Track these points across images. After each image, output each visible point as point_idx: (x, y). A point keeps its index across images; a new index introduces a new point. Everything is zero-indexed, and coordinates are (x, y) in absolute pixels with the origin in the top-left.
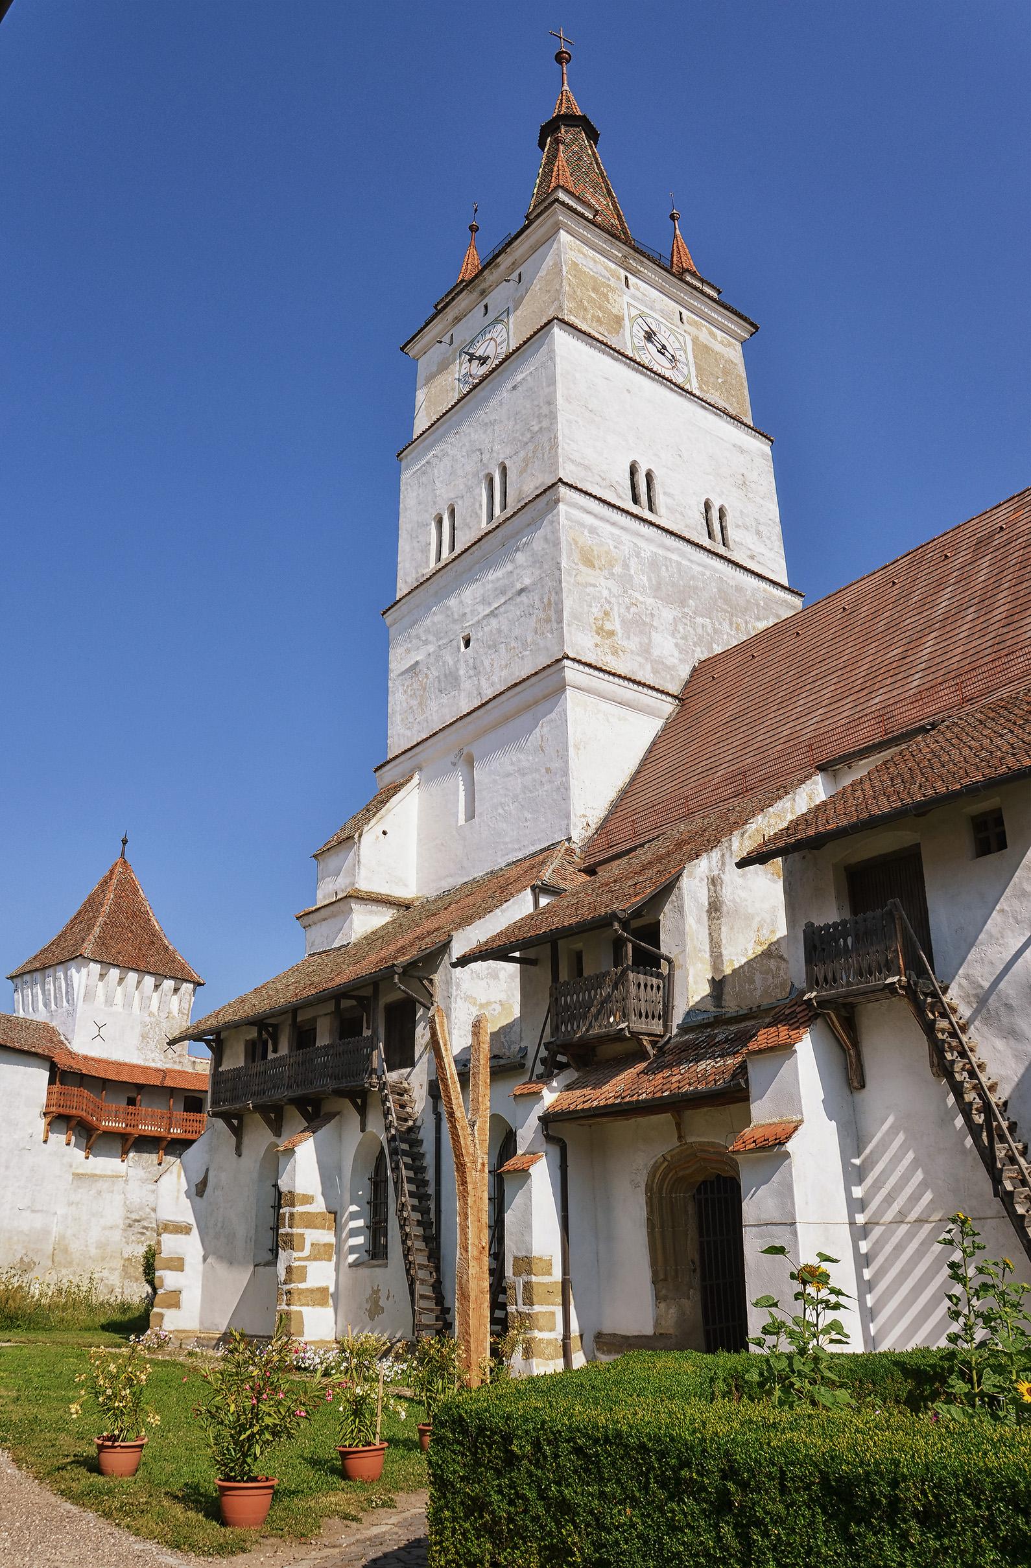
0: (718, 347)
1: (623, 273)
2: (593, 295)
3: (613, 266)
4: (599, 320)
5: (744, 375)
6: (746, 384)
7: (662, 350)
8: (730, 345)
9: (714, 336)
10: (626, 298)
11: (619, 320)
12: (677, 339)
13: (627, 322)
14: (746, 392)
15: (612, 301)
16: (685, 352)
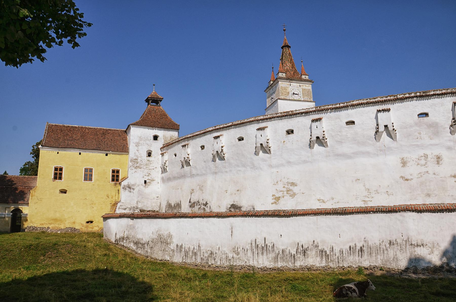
0: (307, 88)
1: (289, 83)
2: (284, 90)
3: (288, 83)
4: (285, 95)
5: (312, 91)
6: (312, 92)
7: (296, 94)
8: (309, 86)
9: (306, 86)
10: (290, 88)
11: (289, 93)
12: (299, 91)
13: (290, 92)
14: (312, 94)
15: (288, 90)
16: (300, 92)
